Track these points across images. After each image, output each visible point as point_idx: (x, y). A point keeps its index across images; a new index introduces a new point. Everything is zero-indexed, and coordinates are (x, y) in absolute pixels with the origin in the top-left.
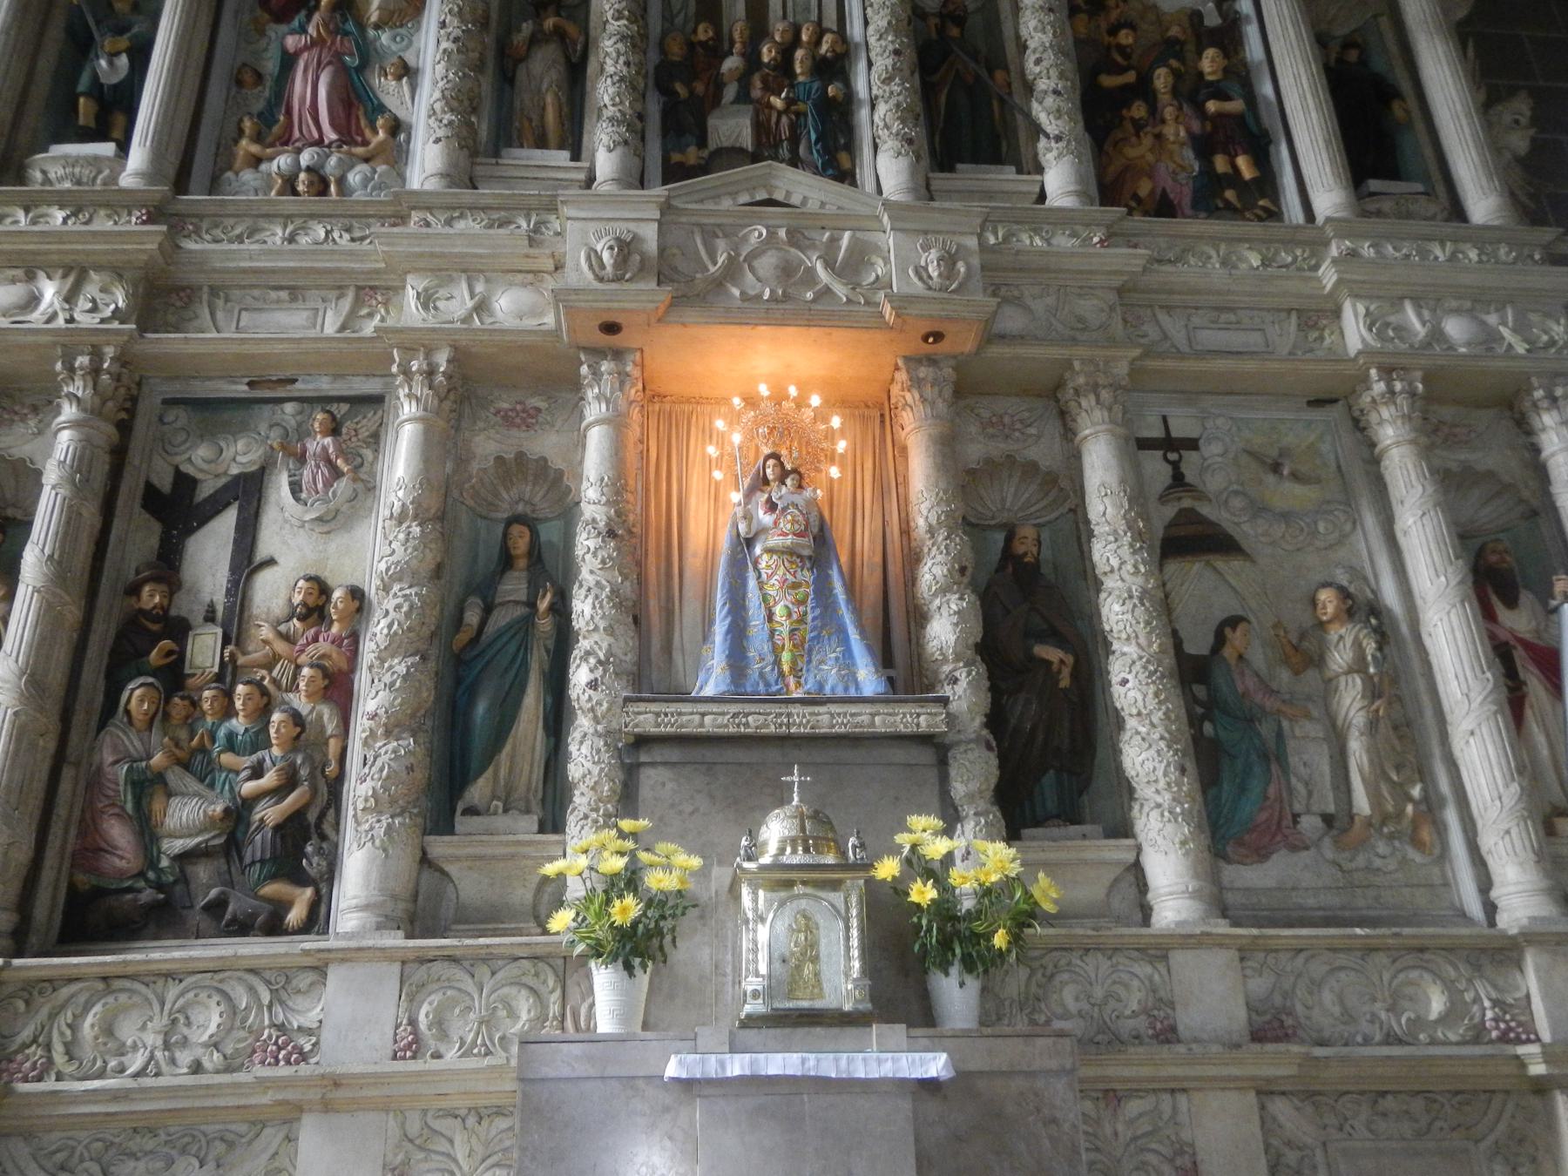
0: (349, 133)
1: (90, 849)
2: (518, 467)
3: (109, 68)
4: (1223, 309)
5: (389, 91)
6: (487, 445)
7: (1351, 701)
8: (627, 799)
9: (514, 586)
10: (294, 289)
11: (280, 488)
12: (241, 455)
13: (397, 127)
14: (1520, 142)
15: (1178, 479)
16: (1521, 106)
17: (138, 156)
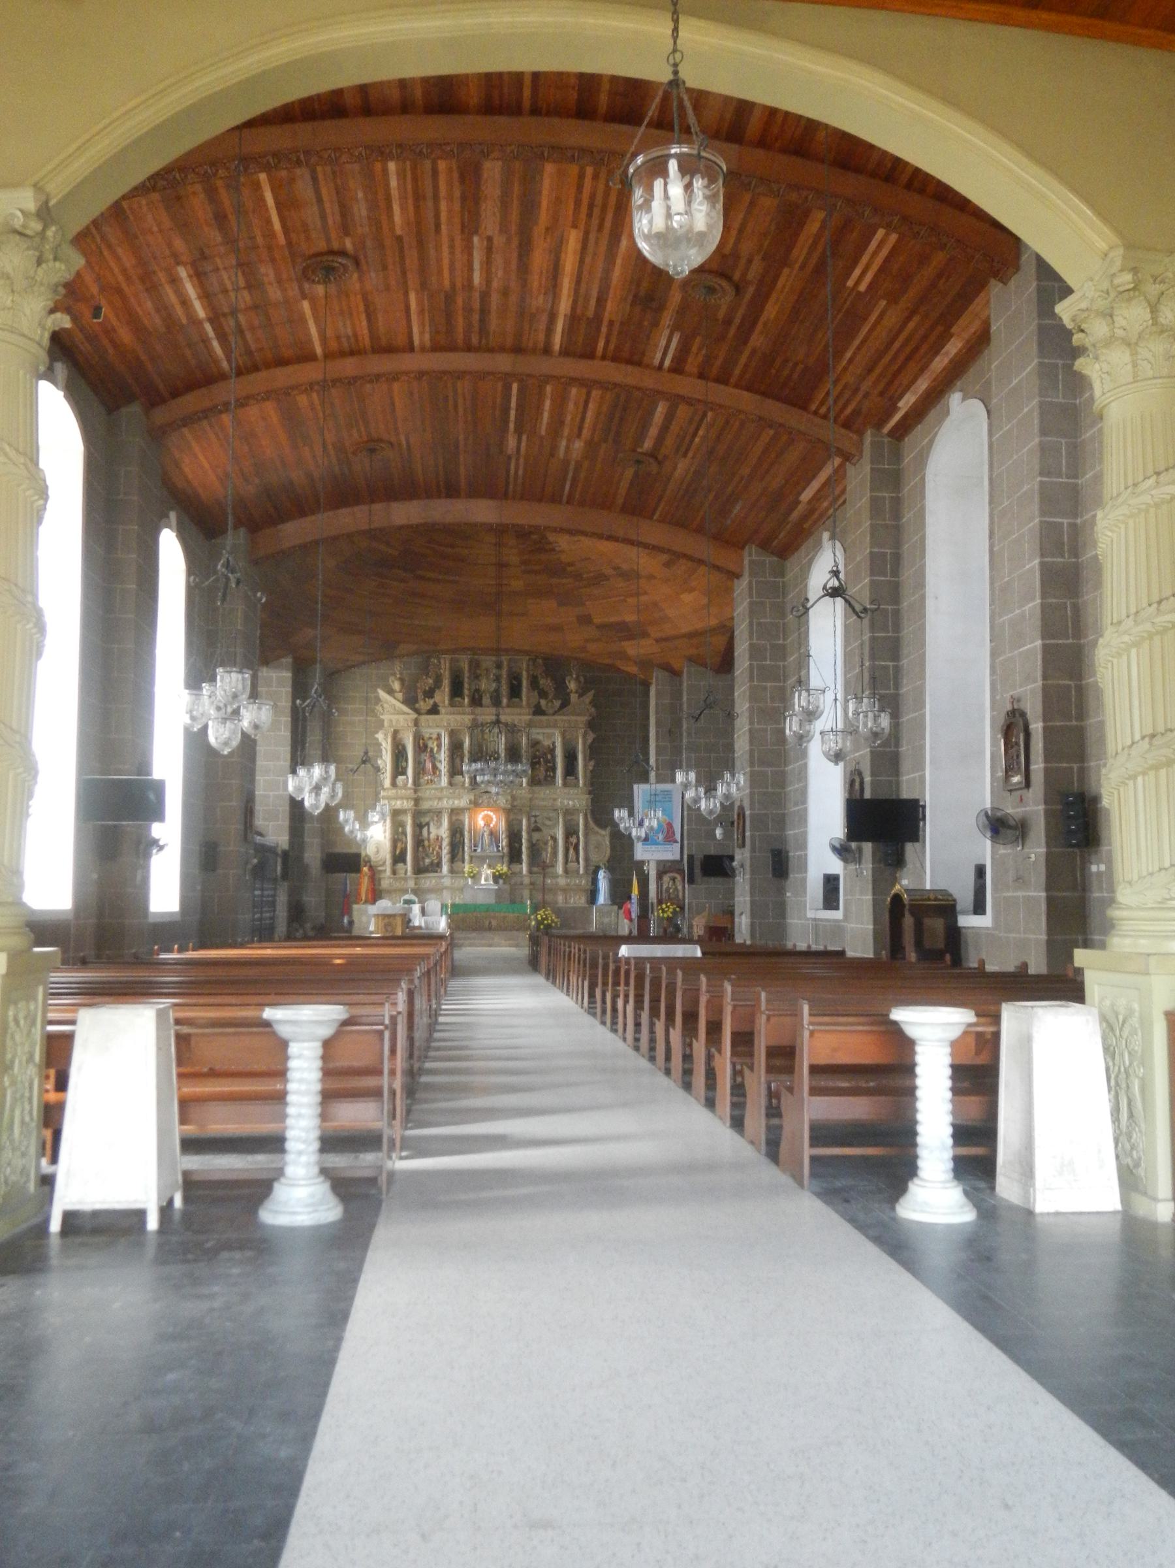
0: (434, 773)
1: (418, 864)
2: (457, 820)
3: (404, 764)
4: (543, 800)
5: (438, 765)
6: (454, 818)
7: (549, 849)
8: (471, 861)
9: (458, 835)
10: (431, 799)
11: (432, 824)
12: (427, 819)
13: (440, 771)
14: (591, 768)
15: (536, 822)
16: (592, 763)
17: (410, 781)
